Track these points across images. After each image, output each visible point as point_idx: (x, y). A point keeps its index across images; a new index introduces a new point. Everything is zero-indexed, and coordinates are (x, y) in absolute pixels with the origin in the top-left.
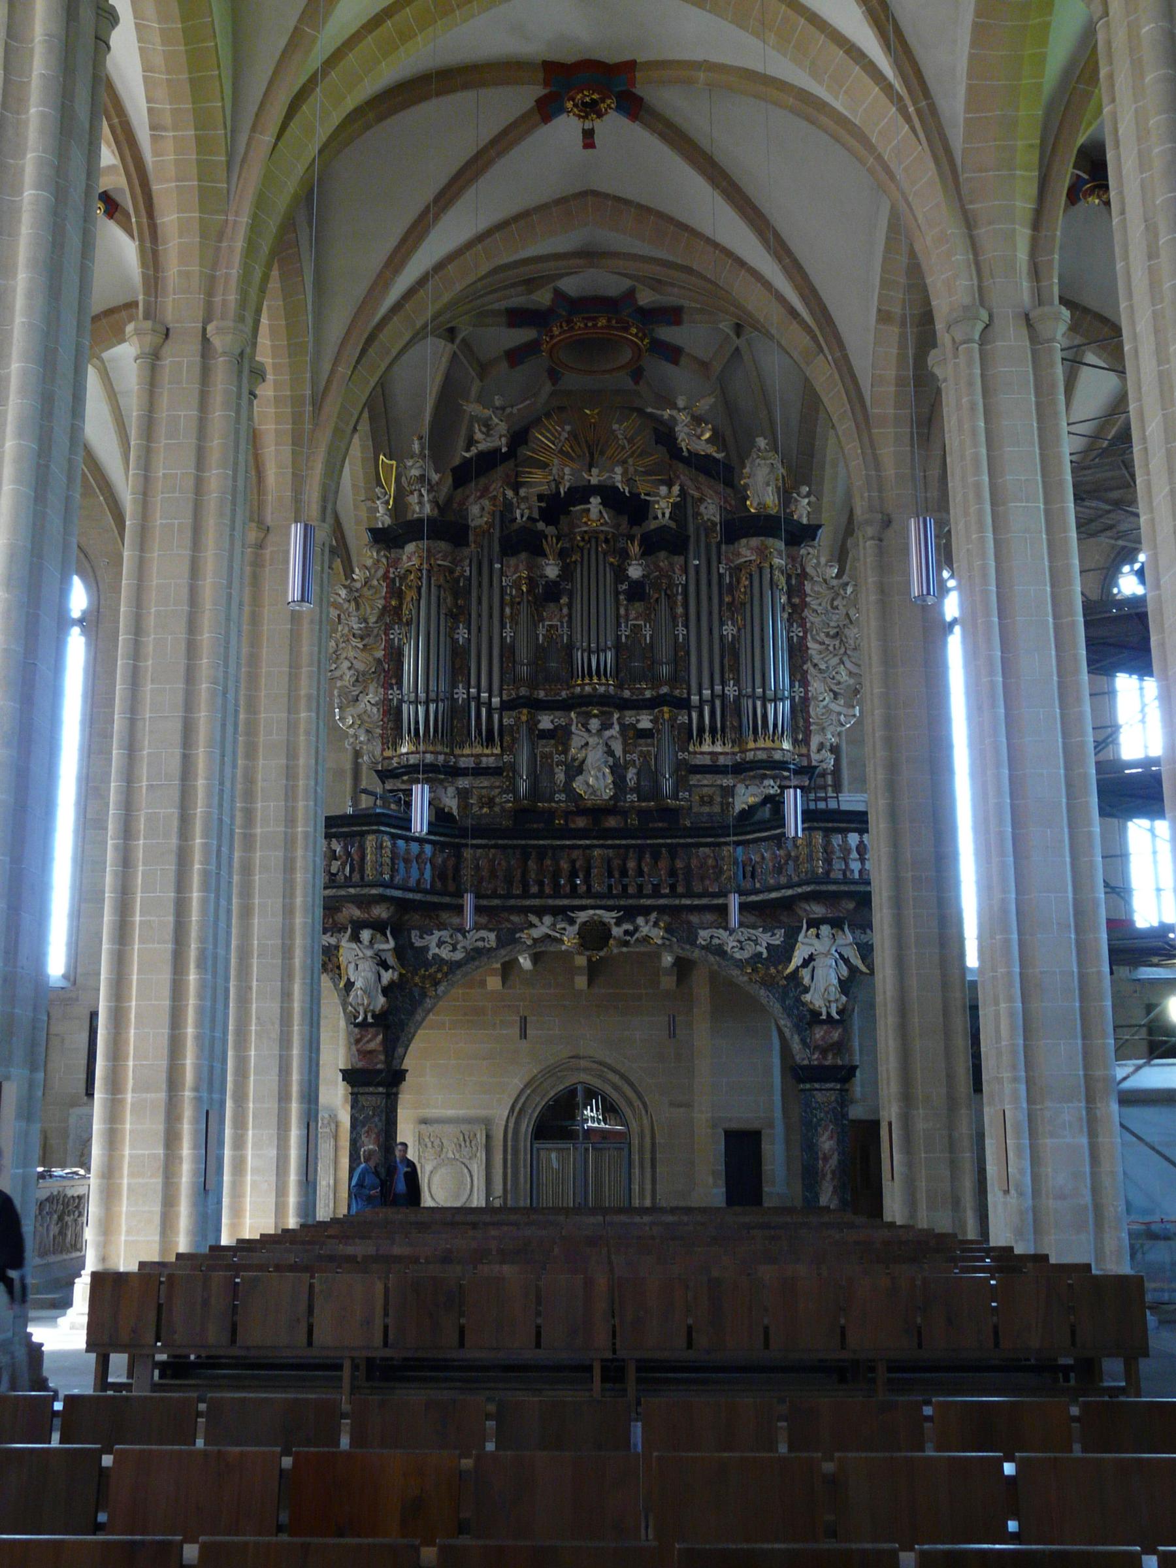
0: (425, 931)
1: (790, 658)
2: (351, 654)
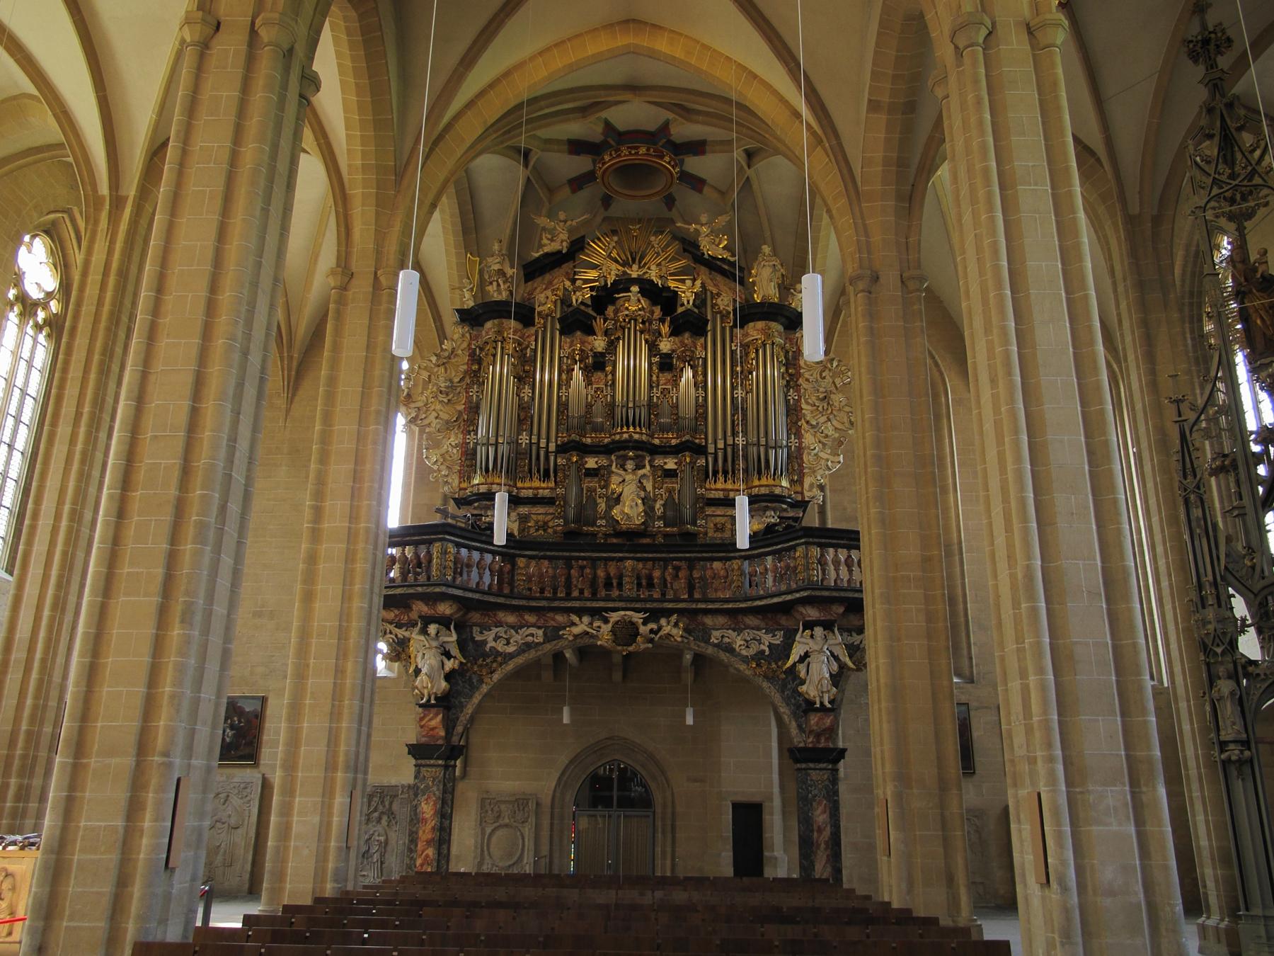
0: (485, 628)
1: (787, 416)
2: (439, 407)
